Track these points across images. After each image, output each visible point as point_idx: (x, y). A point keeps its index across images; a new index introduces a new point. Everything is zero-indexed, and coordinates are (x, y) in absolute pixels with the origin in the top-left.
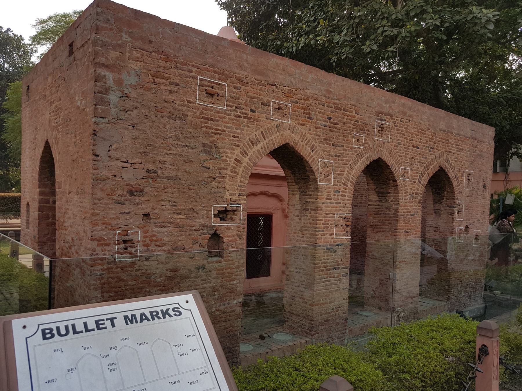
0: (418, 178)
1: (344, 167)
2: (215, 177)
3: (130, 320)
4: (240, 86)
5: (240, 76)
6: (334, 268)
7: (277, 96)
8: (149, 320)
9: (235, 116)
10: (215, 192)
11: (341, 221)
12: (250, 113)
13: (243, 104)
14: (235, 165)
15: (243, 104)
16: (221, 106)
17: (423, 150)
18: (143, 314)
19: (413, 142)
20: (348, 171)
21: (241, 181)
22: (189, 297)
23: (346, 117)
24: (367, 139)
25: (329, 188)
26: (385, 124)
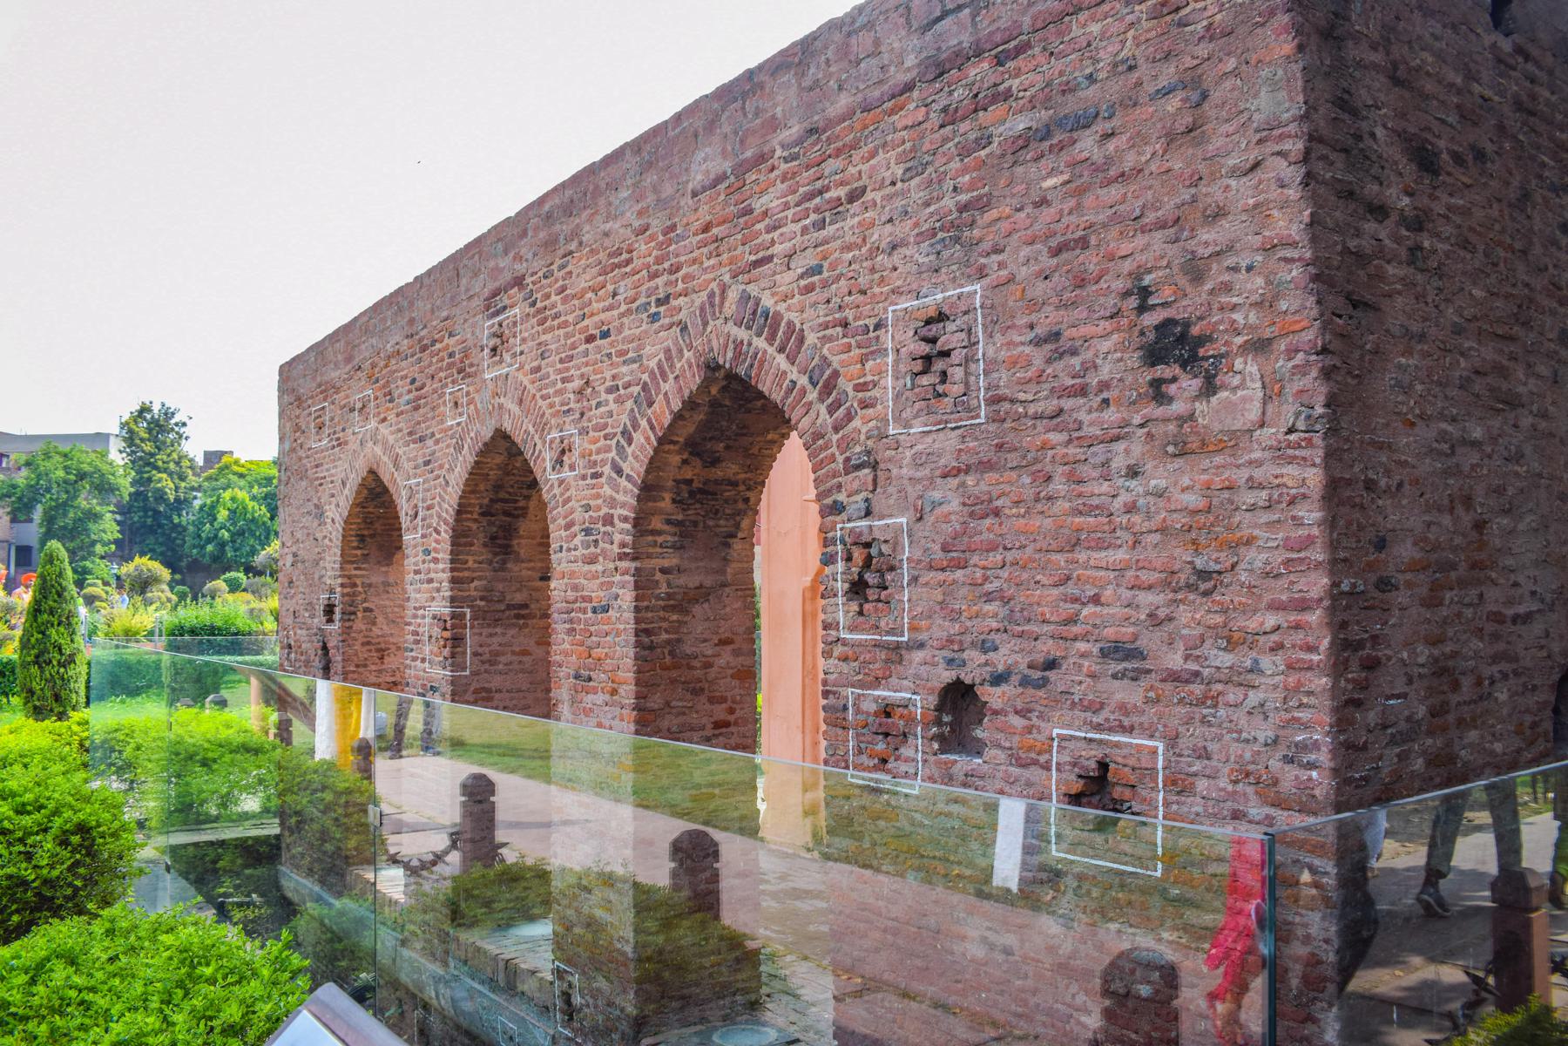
0: (613, 454)
17: (627, 333)
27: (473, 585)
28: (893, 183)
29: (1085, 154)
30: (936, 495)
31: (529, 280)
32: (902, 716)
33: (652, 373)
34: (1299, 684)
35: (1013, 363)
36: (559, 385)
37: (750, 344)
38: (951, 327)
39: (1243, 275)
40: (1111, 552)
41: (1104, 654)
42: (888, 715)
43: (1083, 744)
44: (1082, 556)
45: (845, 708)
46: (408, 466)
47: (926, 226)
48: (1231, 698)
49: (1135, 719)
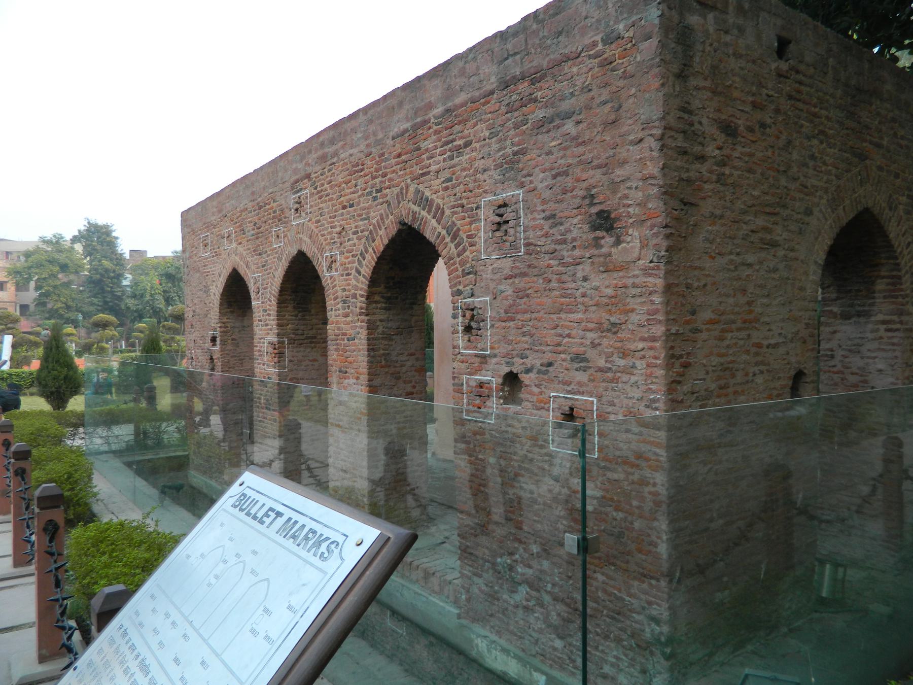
0: (356, 264)
17: (362, 205)
19: (342, 199)
24: (285, 229)
27: (288, 327)
28: (485, 140)
29: (568, 131)
30: (502, 287)
31: (313, 176)
32: (487, 388)
33: (374, 226)
34: (651, 373)
35: (534, 228)
36: (330, 230)
37: (420, 214)
38: (509, 210)
39: (633, 191)
40: (575, 314)
41: (572, 360)
42: (481, 387)
43: (563, 400)
44: (563, 316)
45: (462, 384)
46: (253, 267)
47: (499, 161)
48: (624, 379)
49: (584, 389)
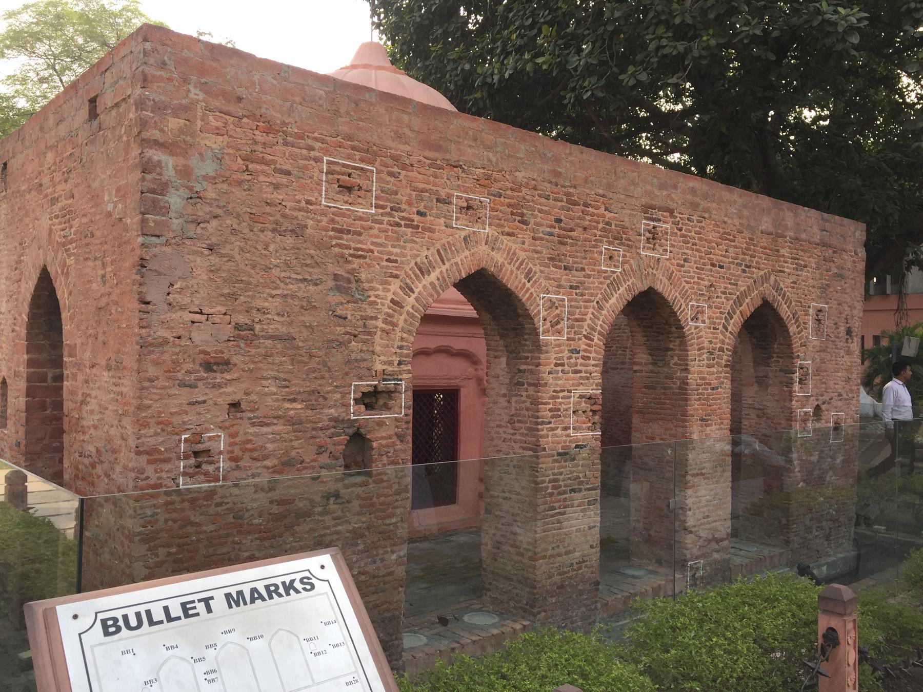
0: (723, 321)
1: (586, 307)
2: (357, 333)
3: (234, 600)
4: (399, 171)
5: (399, 153)
6: (573, 490)
7: (463, 186)
8: (264, 599)
9: (391, 225)
10: (356, 360)
11: (583, 404)
12: (416, 218)
13: (404, 202)
14: (390, 311)
15: (404, 202)
16: (364, 207)
18: (254, 590)
19: (711, 256)
20: (593, 314)
21: (402, 339)
22: (326, 559)
23: (588, 218)
24: (628, 255)
25: (559, 346)
26: (660, 227)
